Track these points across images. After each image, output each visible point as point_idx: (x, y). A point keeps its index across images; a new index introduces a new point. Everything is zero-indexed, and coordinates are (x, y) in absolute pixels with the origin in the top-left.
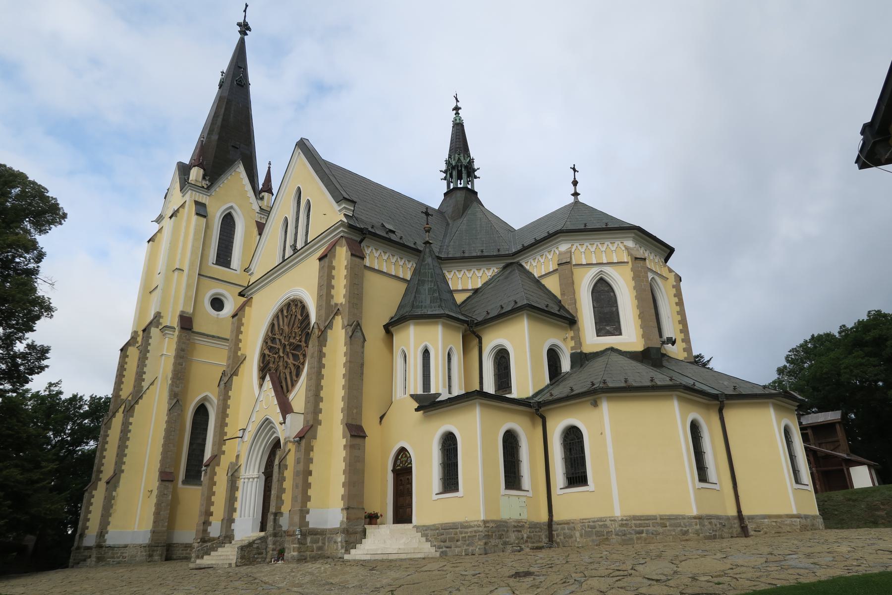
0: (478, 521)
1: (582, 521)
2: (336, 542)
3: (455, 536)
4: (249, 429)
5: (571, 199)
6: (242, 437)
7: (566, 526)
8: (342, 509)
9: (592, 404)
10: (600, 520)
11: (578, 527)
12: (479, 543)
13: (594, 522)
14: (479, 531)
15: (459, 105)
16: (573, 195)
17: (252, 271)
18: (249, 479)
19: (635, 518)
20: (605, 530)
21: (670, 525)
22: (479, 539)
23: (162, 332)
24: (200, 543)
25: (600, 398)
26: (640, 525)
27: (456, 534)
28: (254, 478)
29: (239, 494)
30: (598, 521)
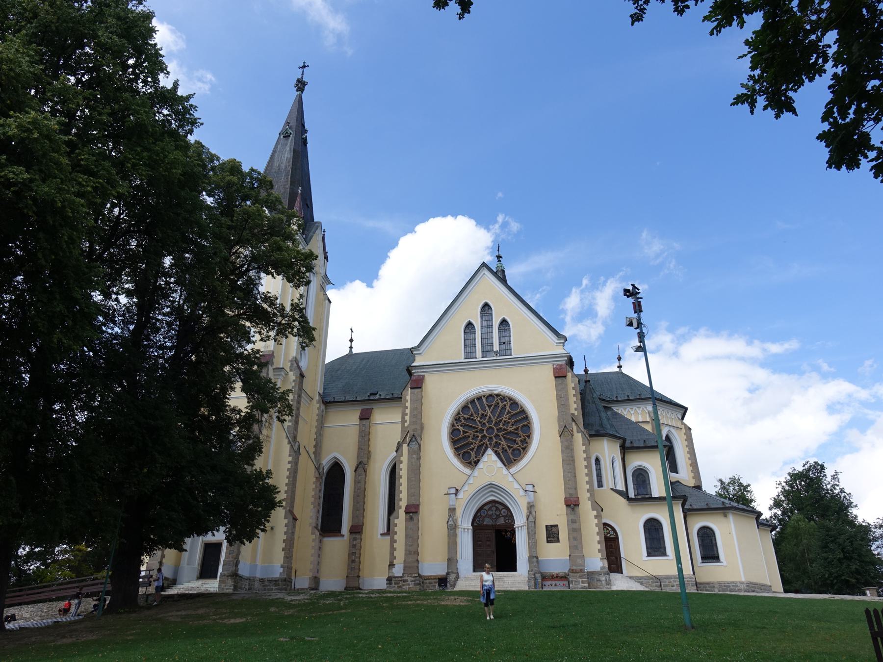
0: (689, 575)
1: (719, 583)
2: (599, 580)
3: (670, 584)
4: (466, 488)
5: (617, 370)
6: (456, 494)
7: (707, 585)
8: (601, 559)
9: (722, 514)
10: (733, 582)
11: (717, 586)
12: (693, 588)
13: (728, 583)
14: (692, 581)
15: (501, 254)
16: (618, 367)
17: (420, 352)
18: (464, 529)
19: (751, 583)
20: (737, 588)
21: (764, 589)
22: (692, 586)
23: (274, 371)
24: (418, 578)
25: (728, 513)
26: (753, 587)
27: (671, 582)
28: (468, 529)
29: (458, 540)
30: (731, 583)
